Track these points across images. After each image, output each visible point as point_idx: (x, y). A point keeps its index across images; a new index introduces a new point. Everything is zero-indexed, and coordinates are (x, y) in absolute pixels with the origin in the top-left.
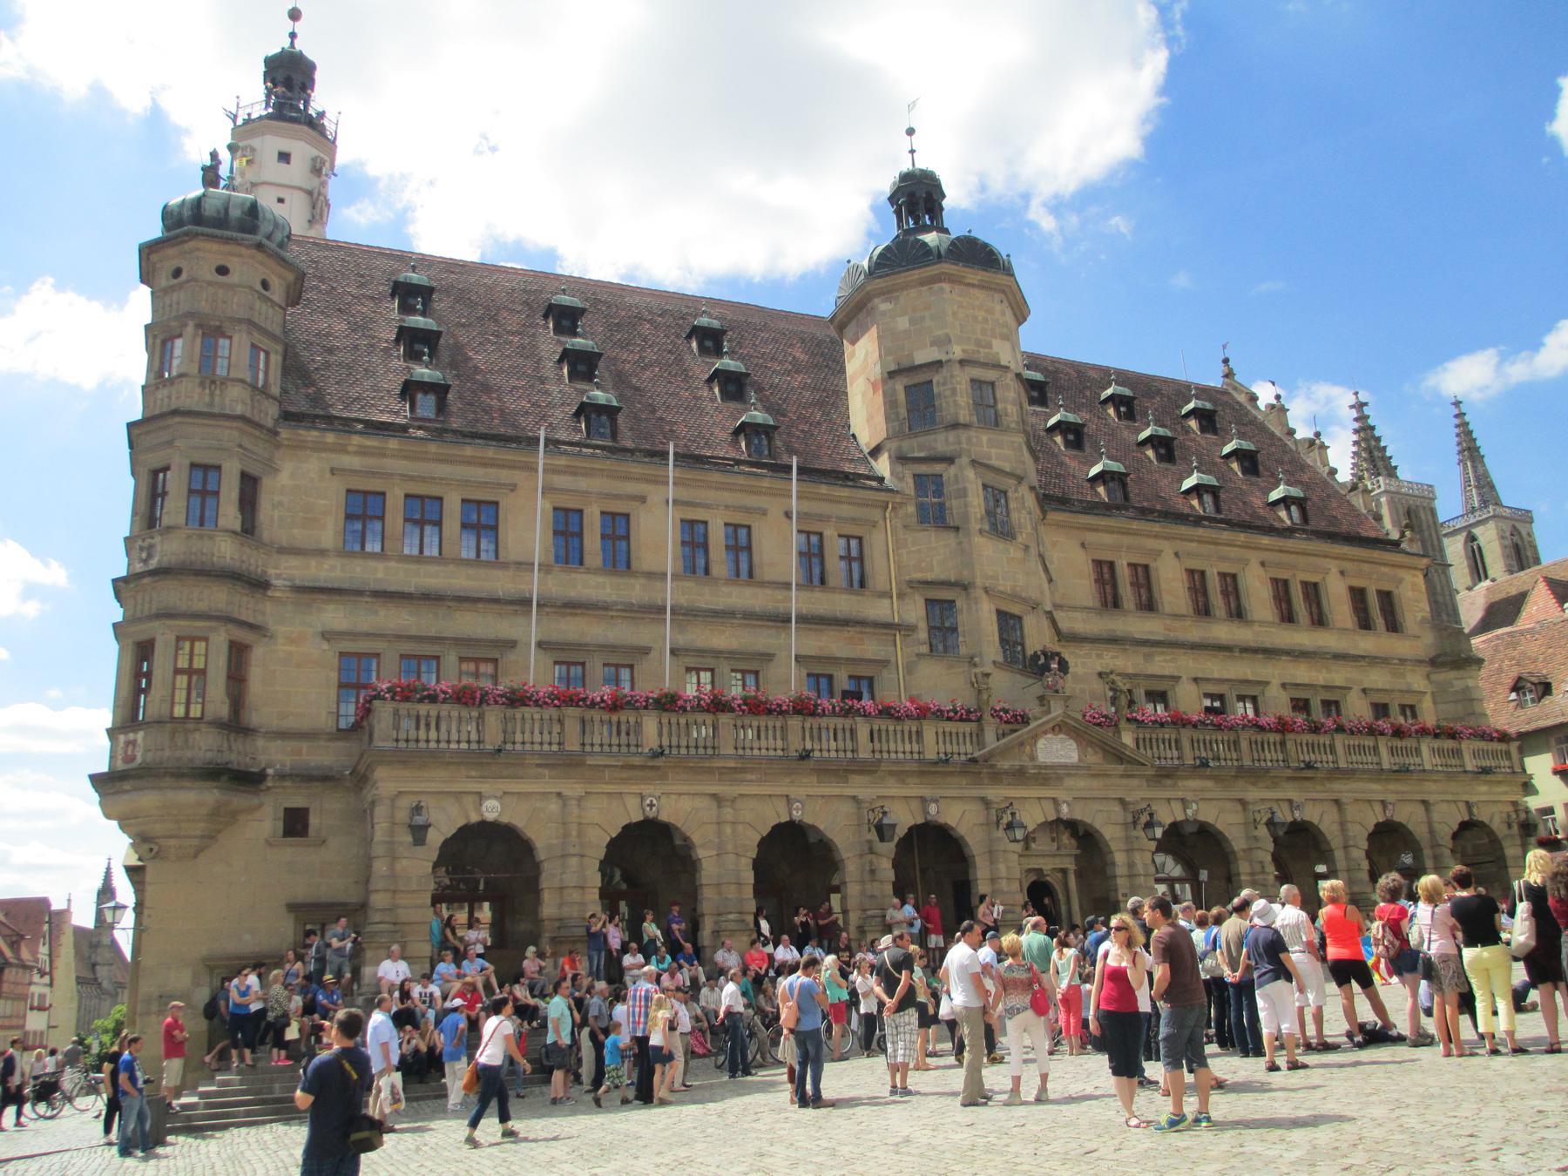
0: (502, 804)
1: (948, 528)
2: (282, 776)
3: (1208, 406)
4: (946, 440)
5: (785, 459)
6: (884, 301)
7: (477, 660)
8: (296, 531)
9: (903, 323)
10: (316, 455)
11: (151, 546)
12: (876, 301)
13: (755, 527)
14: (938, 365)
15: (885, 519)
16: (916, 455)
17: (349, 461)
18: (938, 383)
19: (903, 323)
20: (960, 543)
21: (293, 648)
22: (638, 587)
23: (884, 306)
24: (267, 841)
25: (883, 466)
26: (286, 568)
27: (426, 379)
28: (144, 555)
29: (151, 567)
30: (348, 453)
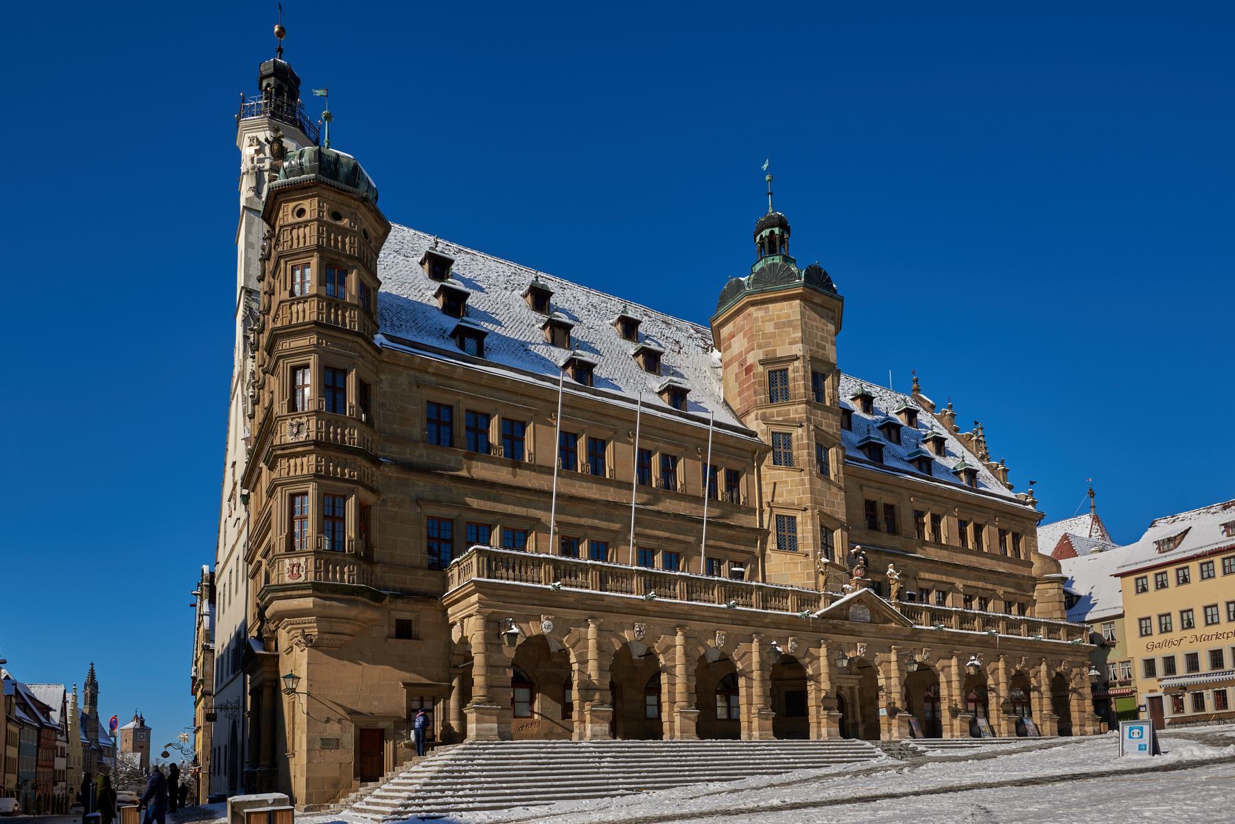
28: (295, 430)
29: (301, 440)
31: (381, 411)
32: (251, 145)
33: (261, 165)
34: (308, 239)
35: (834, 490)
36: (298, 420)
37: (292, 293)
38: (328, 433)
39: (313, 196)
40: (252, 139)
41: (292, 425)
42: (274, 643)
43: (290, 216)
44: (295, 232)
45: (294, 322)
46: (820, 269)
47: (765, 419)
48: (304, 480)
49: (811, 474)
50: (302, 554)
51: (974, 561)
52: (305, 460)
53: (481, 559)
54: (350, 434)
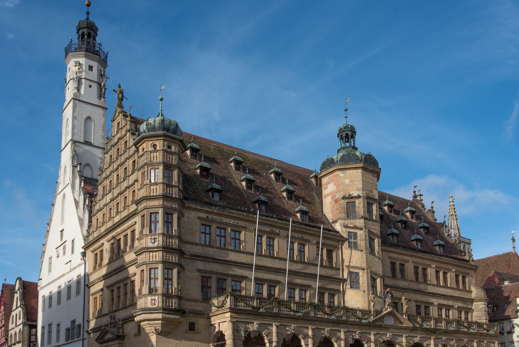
1: (359, 250)
2: (190, 313)
4: (360, 222)
5: (318, 225)
6: (341, 173)
7: (236, 281)
8: (189, 236)
9: (347, 181)
12: (338, 172)
18: (358, 203)
19: (347, 181)
20: (362, 255)
21: (189, 274)
22: (277, 262)
23: (340, 174)
24: (186, 332)
25: (338, 227)
26: (187, 248)
28: (153, 241)
31: (183, 230)
32: (76, 66)
33: (81, 75)
34: (158, 158)
35: (377, 260)
36: (154, 237)
37: (150, 182)
38: (166, 242)
39: (161, 139)
40: (76, 63)
42: (122, 330)
43: (150, 147)
44: (152, 154)
45: (151, 194)
46: (371, 155)
47: (346, 227)
48: (157, 263)
49: (366, 253)
50: (157, 295)
51: (443, 291)
52: (157, 253)
53: (231, 298)
54: (175, 242)
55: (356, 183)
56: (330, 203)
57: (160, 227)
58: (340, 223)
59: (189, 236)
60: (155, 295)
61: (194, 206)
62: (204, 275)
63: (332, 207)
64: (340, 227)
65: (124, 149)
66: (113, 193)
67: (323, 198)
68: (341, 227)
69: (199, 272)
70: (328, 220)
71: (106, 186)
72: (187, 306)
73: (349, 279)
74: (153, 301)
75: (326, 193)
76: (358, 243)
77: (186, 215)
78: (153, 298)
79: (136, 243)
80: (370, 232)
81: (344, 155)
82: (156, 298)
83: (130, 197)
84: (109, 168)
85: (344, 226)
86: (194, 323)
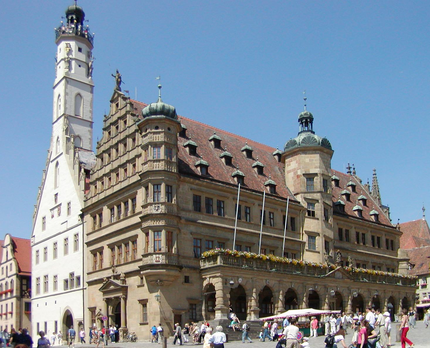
0: (242, 280)
3: (354, 184)
8: (184, 205)
10: (187, 184)
11: (159, 207)
13: (275, 213)
14: (316, 174)
15: (300, 214)
16: (309, 198)
17: (194, 186)
18: (316, 179)
21: (185, 236)
24: (182, 283)
25: (299, 198)
27: (204, 164)
28: (157, 208)
30: (194, 184)
31: (179, 199)
41: (155, 207)
47: (305, 199)
55: (314, 162)
56: (293, 178)
57: (163, 197)
58: (301, 196)
59: (184, 205)
60: (159, 254)
61: (188, 179)
62: (196, 237)
63: (294, 181)
64: (301, 198)
65: (123, 127)
66: (112, 165)
67: (286, 173)
68: (302, 199)
69: (192, 235)
70: (290, 192)
71: (105, 158)
72: (183, 262)
73: (307, 242)
74: (158, 259)
75: (289, 169)
76: (315, 212)
77: (181, 186)
78: (157, 255)
79: (138, 209)
80: (324, 203)
81: (305, 138)
82: (160, 256)
83: (130, 169)
84: (108, 142)
85: (304, 198)
86: (188, 277)
